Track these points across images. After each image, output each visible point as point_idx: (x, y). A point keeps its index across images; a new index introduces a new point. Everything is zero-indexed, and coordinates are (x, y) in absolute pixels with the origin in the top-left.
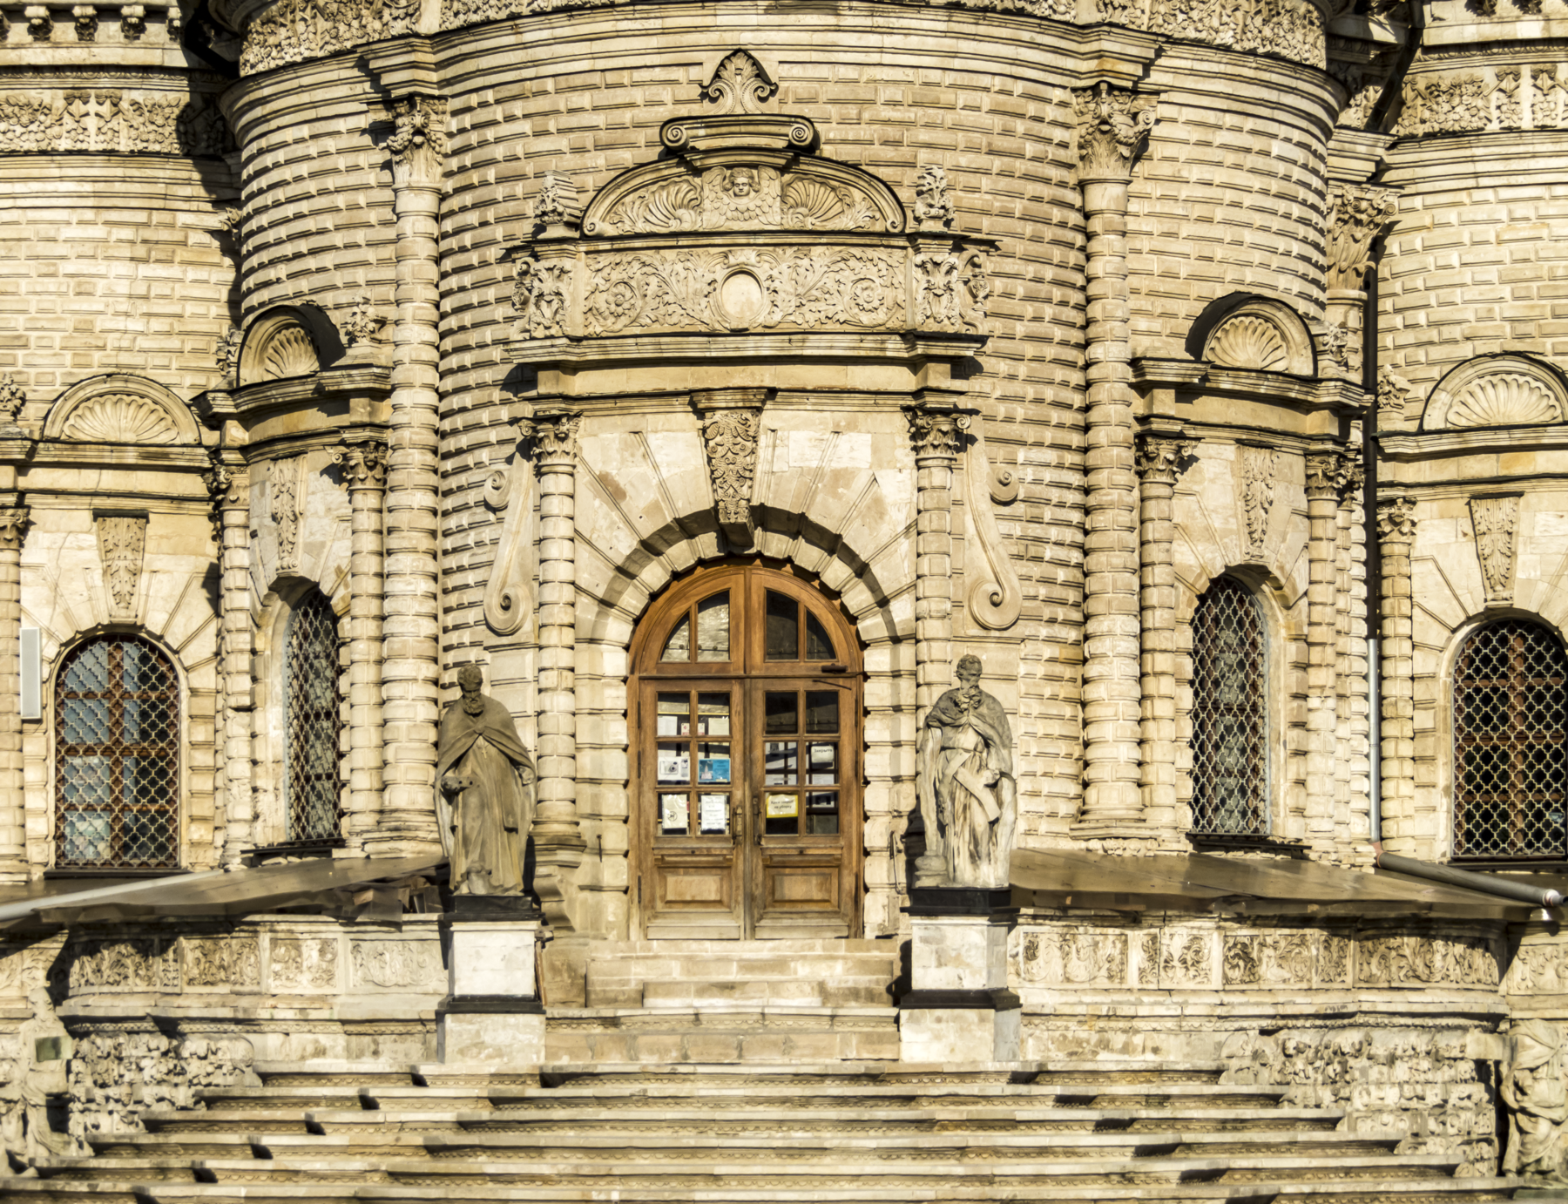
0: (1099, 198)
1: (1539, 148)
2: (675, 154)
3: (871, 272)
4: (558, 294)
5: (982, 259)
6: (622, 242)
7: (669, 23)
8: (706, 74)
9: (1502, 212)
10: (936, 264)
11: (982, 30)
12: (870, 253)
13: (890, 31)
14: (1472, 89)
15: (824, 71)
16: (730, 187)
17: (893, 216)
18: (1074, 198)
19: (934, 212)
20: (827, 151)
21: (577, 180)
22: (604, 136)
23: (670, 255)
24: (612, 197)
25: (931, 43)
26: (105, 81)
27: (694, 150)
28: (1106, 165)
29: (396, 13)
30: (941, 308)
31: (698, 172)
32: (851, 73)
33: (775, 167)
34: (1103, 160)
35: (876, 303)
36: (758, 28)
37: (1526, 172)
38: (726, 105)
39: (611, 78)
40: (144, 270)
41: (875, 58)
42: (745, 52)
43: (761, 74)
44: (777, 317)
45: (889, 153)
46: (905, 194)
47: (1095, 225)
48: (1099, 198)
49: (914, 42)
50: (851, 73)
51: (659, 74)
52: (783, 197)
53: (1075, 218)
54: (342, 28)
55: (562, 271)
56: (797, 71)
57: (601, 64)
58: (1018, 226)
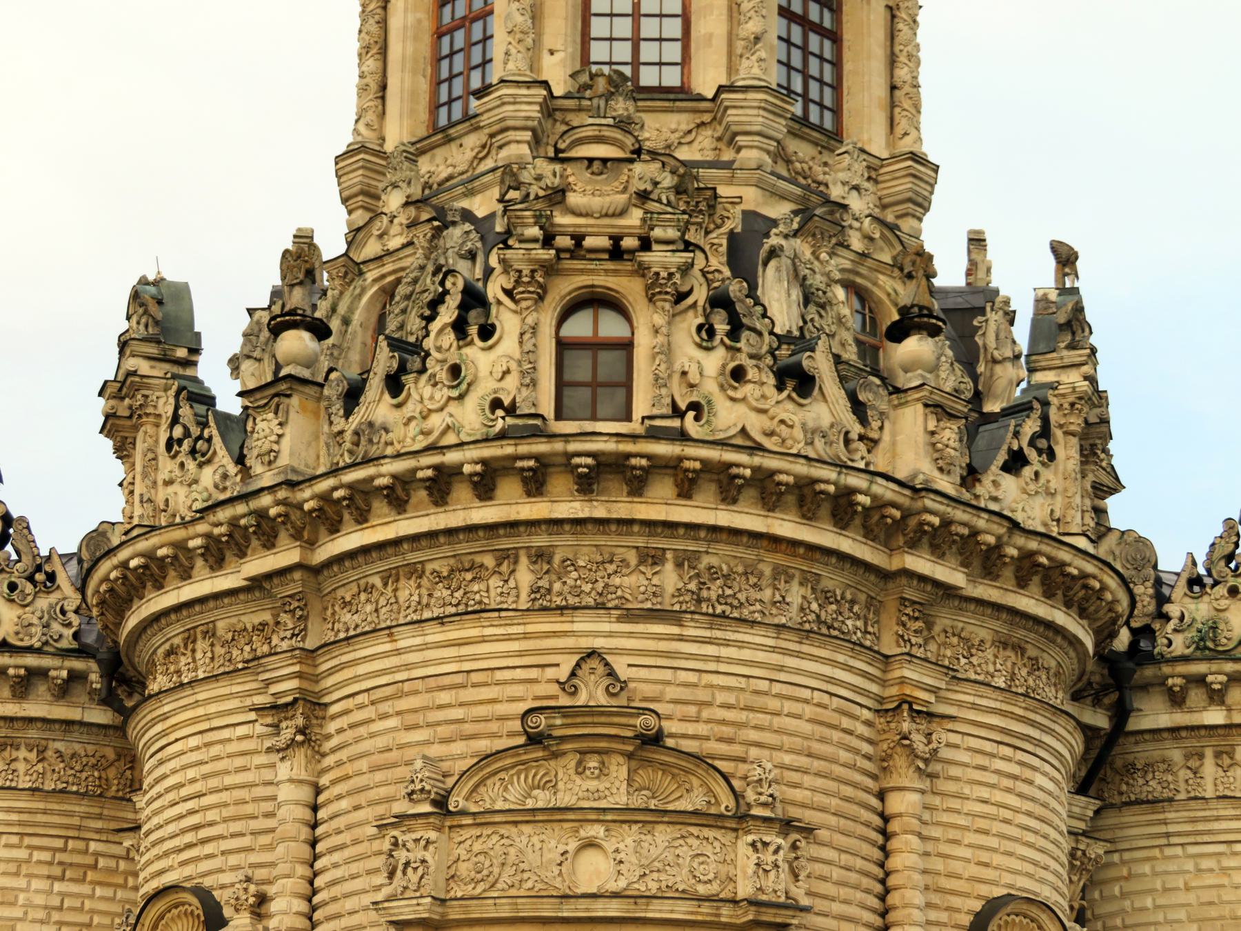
0: (896, 803)
1: (1222, 813)
2: (535, 739)
3: (708, 850)
4: (423, 861)
5: (802, 844)
6: (484, 819)
7: (530, 628)
8: (563, 673)
9: (1190, 865)
10: (765, 844)
11: (805, 648)
12: (707, 832)
13: (727, 643)
14: (1163, 767)
15: (667, 675)
16: (580, 770)
17: (726, 802)
18: (874, 802)
19: (763, 799)
20: (670, 742)
21: (445, 766)
22: (469, 728)
23: (527, 829)
24: (475, 779)
25: (761, 656)
26: (33, 733)
27: (550, 736)
28: (903, 774)
29: (282, 634)
30: (770, 882)
31: (555, 755)
32: (692, 678)
33: (622, 753)
34: (903, 771)
35: (711, 876)
36: (611, 634)
37: (1209, 832)
38: (582, 699)
39: (475, 677)
40: (57, 886)
41: (712, 666)
42: (599, 655)
43: (611, 674)
44: (622, 884)
45: (723, 748)
46: (736, 784)
47: (894, 826)
48: (896, 803)
49: (746, 654)
50: (692, 678)
51: (519, 674)
52: (630, 781)
53: (877, 821)
54: (235, 652)
55: (428, 842)
56: (643, 673)
57: (467, 666)
58: (833, 820)
